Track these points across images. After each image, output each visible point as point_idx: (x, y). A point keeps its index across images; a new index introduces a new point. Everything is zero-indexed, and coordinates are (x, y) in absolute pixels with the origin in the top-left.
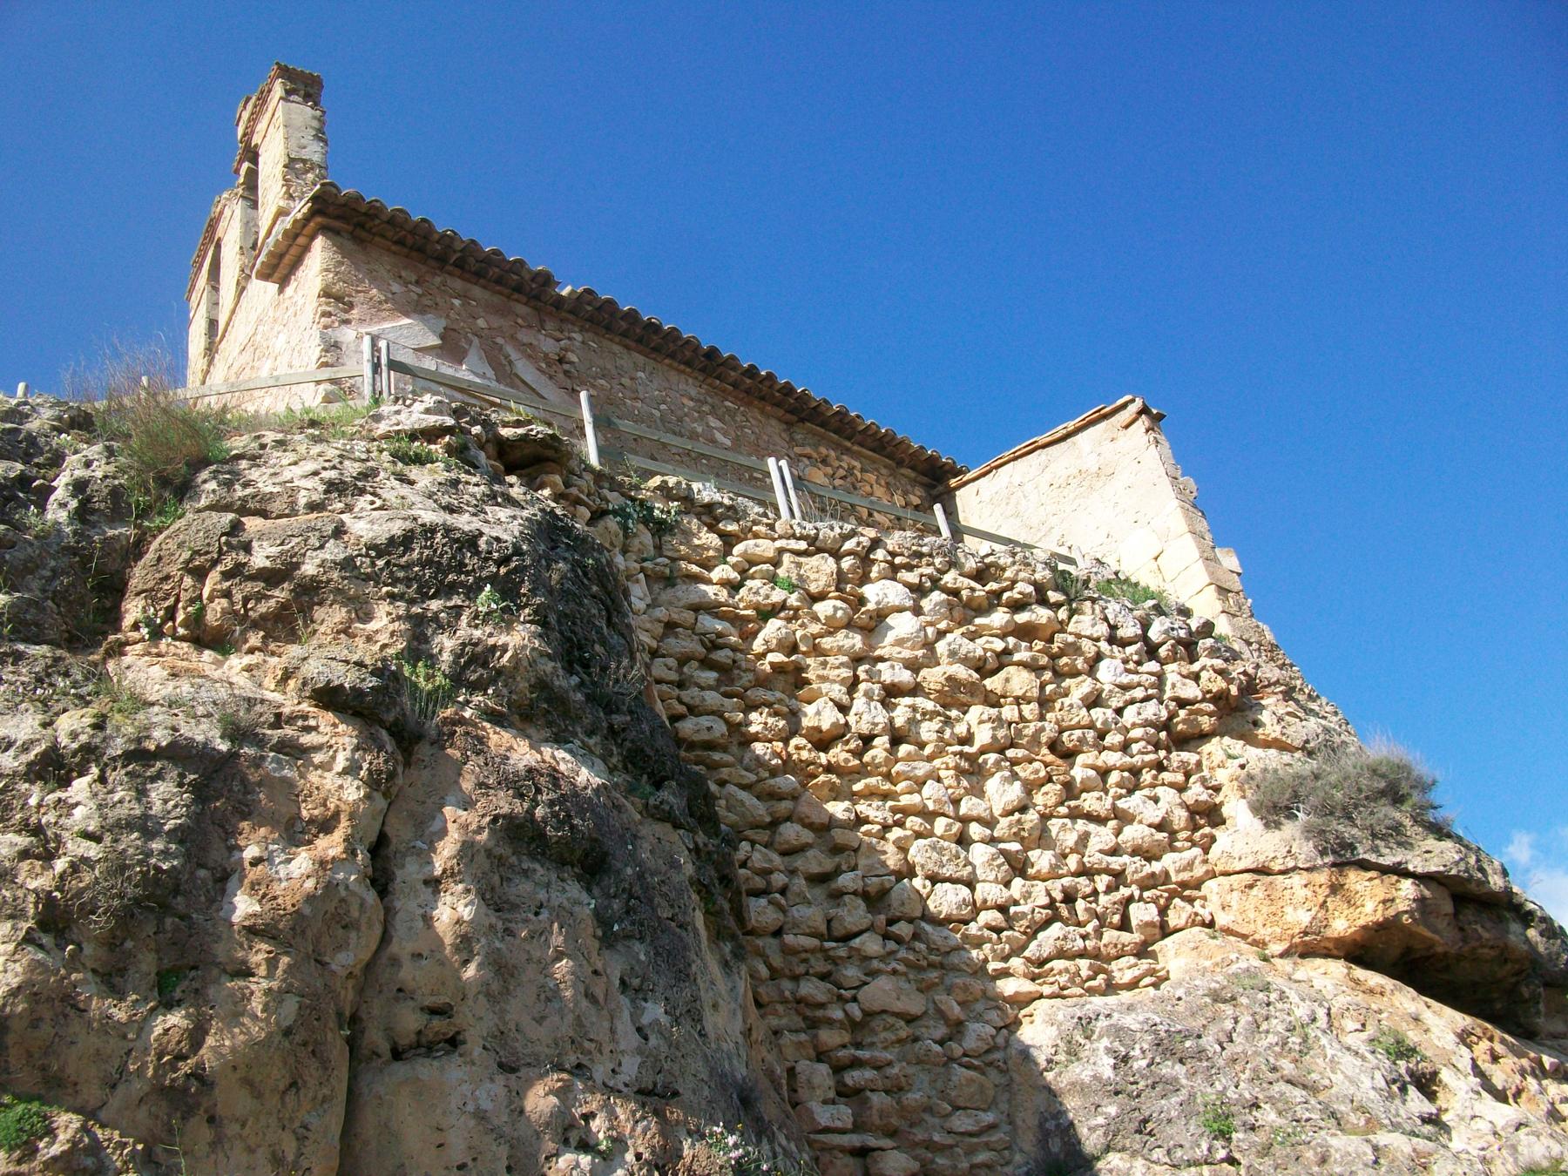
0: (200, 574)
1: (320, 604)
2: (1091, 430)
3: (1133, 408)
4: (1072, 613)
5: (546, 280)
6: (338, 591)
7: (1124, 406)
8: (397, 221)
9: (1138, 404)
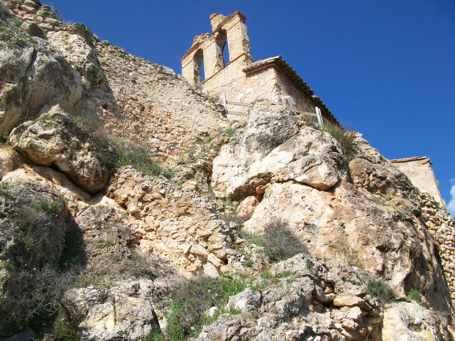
0: (369, 174)
1: (390, 187)
2: (413, 162)
3: (426, 160)
4: (437, 211)
5: (312, 93)
6: (393, 185)
7: (424, 159)
8: (289, 69)
9: (428, 159)
